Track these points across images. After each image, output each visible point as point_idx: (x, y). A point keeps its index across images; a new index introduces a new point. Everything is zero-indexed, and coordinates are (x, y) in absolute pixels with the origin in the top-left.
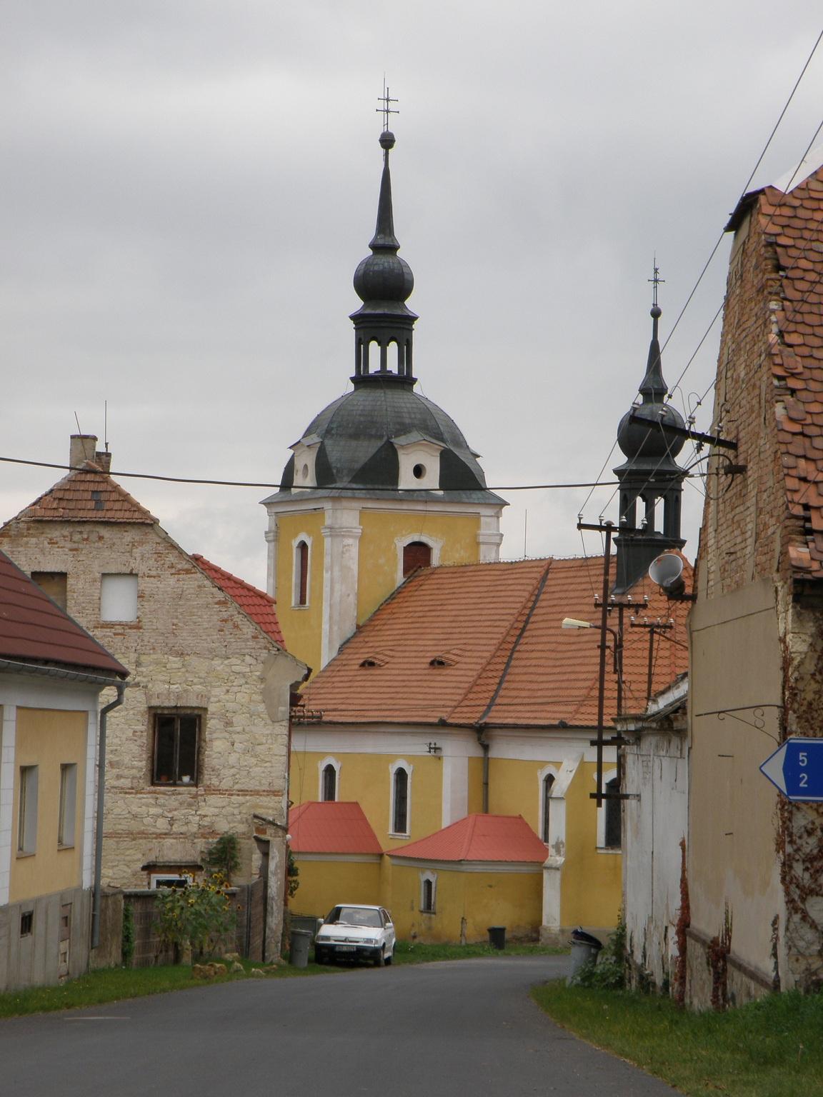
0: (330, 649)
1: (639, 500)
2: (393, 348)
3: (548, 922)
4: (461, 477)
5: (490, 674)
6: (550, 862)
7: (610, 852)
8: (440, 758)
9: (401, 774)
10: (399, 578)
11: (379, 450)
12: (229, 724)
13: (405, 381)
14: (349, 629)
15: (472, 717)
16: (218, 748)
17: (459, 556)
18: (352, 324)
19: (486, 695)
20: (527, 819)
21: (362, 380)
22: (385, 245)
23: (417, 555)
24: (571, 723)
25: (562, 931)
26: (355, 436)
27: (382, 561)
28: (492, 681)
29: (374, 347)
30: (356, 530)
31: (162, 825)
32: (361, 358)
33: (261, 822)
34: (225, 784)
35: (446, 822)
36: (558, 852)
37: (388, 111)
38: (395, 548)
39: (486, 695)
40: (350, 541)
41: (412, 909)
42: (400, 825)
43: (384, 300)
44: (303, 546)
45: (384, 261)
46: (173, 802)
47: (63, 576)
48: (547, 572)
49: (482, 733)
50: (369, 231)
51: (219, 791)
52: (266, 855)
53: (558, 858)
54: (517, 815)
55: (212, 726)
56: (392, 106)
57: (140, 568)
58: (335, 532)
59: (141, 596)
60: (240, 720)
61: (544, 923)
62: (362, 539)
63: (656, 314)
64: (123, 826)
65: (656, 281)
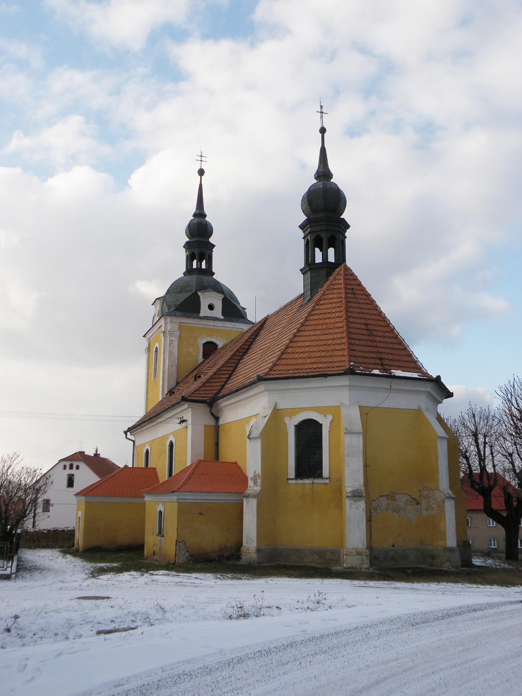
0: (162, 395)
1: (317, 250)
3: (247, 543)
5: (223, 372)
7: (300, 481)
8: (186, 427)
10: (201, 359)
11: (191, 296)
14: (173, 384)
18: (184, 250)
22: (200, 213)
23: (210, 348)
25: (259, 550)
26: (180, 292)
27: (191, 350)
28: (224, 376)
30: (176, 333)
36: (255, 483)
37: (201, 161)
38: (198, 344)
40: (174, 339)
41: (154, 533)
43: (199, 238)
44: (157, 348)
50: (193, 208)
53: (255, 488)
54: (233, 461)
56: (203, 159)
61: (244, 544)
63: (323, 131)
65: (322, 112)
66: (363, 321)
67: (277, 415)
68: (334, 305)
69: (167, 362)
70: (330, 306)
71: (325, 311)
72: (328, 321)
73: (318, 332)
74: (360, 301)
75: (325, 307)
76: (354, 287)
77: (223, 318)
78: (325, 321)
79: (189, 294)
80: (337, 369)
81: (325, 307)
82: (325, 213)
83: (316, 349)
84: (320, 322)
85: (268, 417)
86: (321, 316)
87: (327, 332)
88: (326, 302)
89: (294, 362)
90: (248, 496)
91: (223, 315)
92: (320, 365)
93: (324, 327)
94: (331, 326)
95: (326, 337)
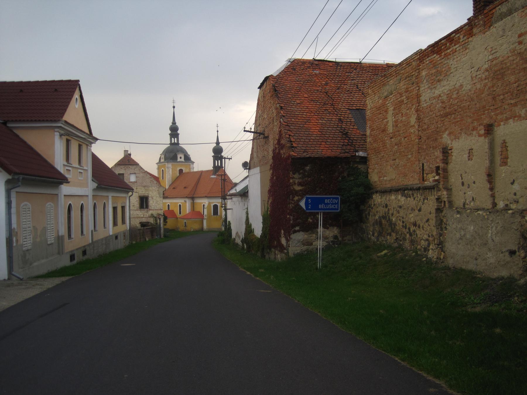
2: (176, 139)
4: (187, 158)
9: (180, 205)
10: (178, 174)
12: (153, 198)
13: (178, 144)
15: (191, 196)
16: (151, 203)
17: (187, 171)
22: (174, 123)
23: (181, 171)
29: (173, 139)
31: (142, 216)
32: (171, 140)
33: (159, 215)
34: (153, 208)
35: (188, 212)
42: (180, 213)
43: (174, 131)
45: (174, 126)
46: (144, 212)
47: (123, 174)
49: (193, 198)
51: (151, 210)
52: (160, 220)
55: (150, 199)
57: (136, 172)
58: (168, 168)
59: (137, 177)
60: (154, 198)
63: (218, 131)
64: (136, 216)
67: (209, 203)
79: (173, 154)
82: (218, 152)
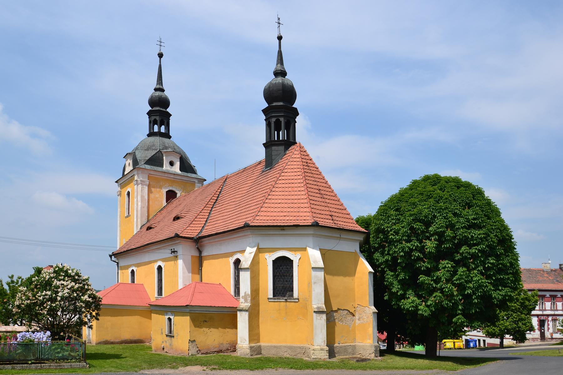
5: (201, 217)
6: (242, 307)
13: (167, 135)
15: (194, 235)
19: (200, 225)
20: (224, 285)
21: (151, 134)
24: (251, 224)
26: (147, 150)
27: (157, 196)
28: (202, 220)
36: (246, 301)
39: (200, 225)
41: (162, 333)
48: (226, 179)
53: (246, 304)
62: (149, 186)
66: (317, 187)
68: (296, 174)
69: (139, 204)
70: (292, 174)
71: (289, 178)
72: (293, 185)
73: (287, 193)
74: (313, 172)
75: (289, 174)
76: (308, 161)
77: (180, 172)
78: (290, 185)
79: (154, 153)
80: (304, 221)
81: (289, 174)
83: (286, 205)
84: (287, 185)
85: (254, 253)
86: (287, 181)
87: (293, 193)
88: (289, 171)
89: (272, 214)
90: (241, 310)
91: (181, 170)
92: (291, 218)
93: (290, 189)
94: (296, 189)
95: (293, 197)
